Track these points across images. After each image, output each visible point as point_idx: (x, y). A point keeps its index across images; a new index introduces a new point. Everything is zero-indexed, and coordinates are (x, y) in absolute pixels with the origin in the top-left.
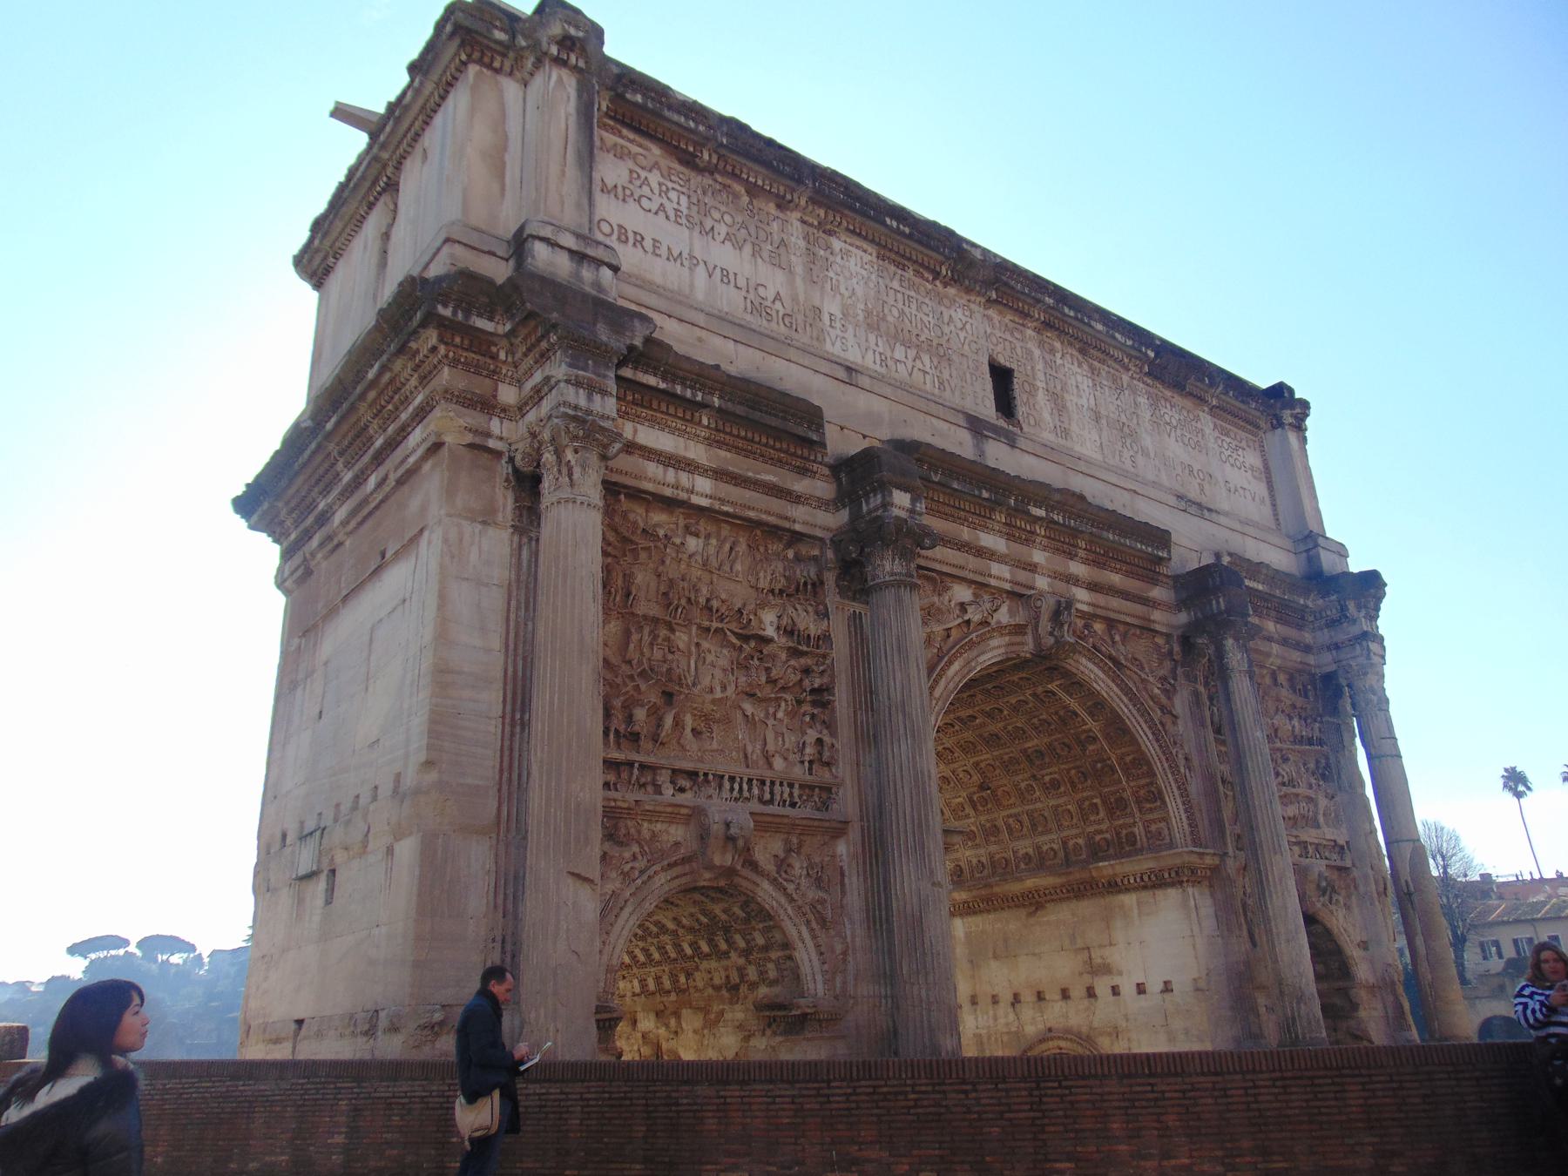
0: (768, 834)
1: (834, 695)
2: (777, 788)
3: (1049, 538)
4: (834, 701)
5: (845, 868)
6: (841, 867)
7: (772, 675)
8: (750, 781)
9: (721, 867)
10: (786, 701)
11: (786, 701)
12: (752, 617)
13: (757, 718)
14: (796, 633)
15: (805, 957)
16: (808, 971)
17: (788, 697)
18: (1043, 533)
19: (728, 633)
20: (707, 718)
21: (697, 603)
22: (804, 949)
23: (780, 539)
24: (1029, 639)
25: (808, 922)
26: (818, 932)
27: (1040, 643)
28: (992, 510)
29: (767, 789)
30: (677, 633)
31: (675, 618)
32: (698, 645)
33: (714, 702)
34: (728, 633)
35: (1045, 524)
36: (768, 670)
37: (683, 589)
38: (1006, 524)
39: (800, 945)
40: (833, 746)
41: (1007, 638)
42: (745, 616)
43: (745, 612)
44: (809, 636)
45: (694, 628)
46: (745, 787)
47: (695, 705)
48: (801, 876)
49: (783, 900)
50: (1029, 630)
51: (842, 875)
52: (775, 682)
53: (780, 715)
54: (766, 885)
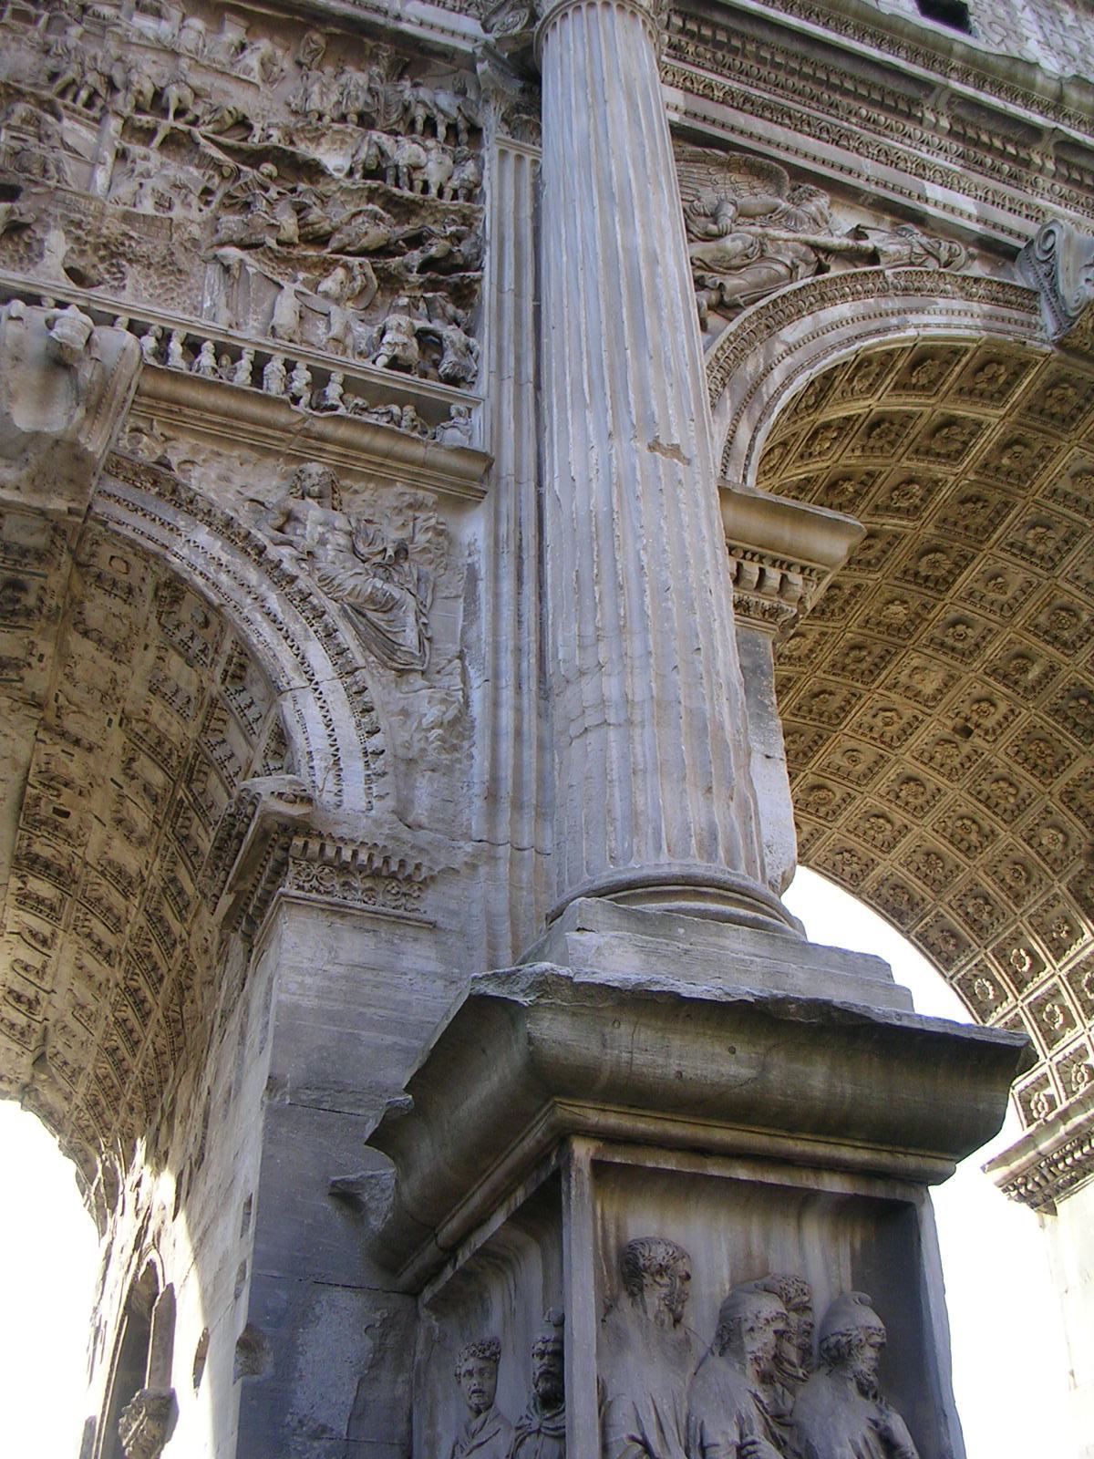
0: (236, 453)
1: (480, 268)
2: (275, 368)
3: (1068, 180)
4: (482, 277)
5: (483, 569)
6: (471, 567)
7: (311, 218)
8: (193, 347)
9: (36, 436)
10: (346, 266)
11: (346, 266)
12: (276, 134)
13: (251, 270)
14: (391, 172)
15: (312, 711)
16: (319, 742)
17: (355, 261)
18: (1050, 165)
19: (203, 141)
20: (114, 253)
21: (128, 85)
22: (311, 696)
23: (374, 58)
24: (1047, 319)
25: (330, 634)
26: (374, 694)
27: (1065, 313)
28: (917, 103)
29: (245, 364)
30: (66, 123)
31: (74, 100)
32: (122, 155)
33: (128, 218)
34: (203, 141)
35: (1051, 150)
36: (300, 209)
37: (95, 59)
38: (951, 133)
39: (299, 681)
40: (469, 349)
41: (986, 307)
42: (257, 132)
43: (257, 127)
44: (426, 183)
45: (114, 125)
46: (176, 347)
47: (77, 216)
48: (323, 542)
49: (253, 576)
50: (1043, 305)
51: (473, 577)
52: (321, 240)
53: (329, 284)
54: (203, 536)
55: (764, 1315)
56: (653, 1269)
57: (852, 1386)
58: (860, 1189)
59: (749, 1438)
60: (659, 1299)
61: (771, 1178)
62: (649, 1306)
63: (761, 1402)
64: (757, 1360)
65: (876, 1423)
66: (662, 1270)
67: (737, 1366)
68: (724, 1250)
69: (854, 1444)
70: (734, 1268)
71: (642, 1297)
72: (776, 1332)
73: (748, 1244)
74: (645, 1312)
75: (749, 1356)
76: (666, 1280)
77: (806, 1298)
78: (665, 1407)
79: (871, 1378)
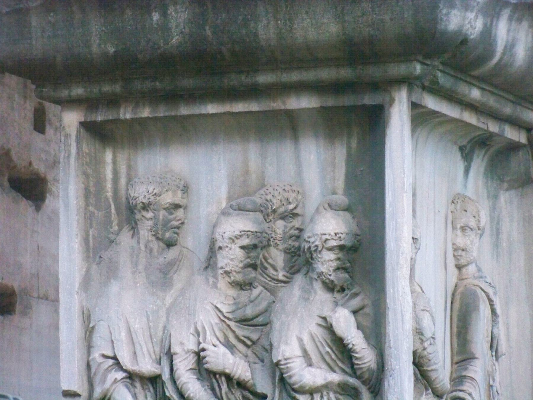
55: (226, 235)
56: (139, 207)
57: (318, 286)
58: (330, 101)
59: (201, 346)
60: (147, 229)
61: (240, 107)
62: (141, 237)
63: (220, 311)
64: (227, 273)
65: (324, 319)
66: (145, 207)
67: (211, 280)
68: (223, 171)
69: (300, 340)
70: (231, 185)
71: (138, 230)
72: (242, 248)
73: (246, 163)
74: (139, 243)
75: (221, 271)
76: (150, 215)
77: (291, 207)
78: (138, 325)
79: (332, 278)
